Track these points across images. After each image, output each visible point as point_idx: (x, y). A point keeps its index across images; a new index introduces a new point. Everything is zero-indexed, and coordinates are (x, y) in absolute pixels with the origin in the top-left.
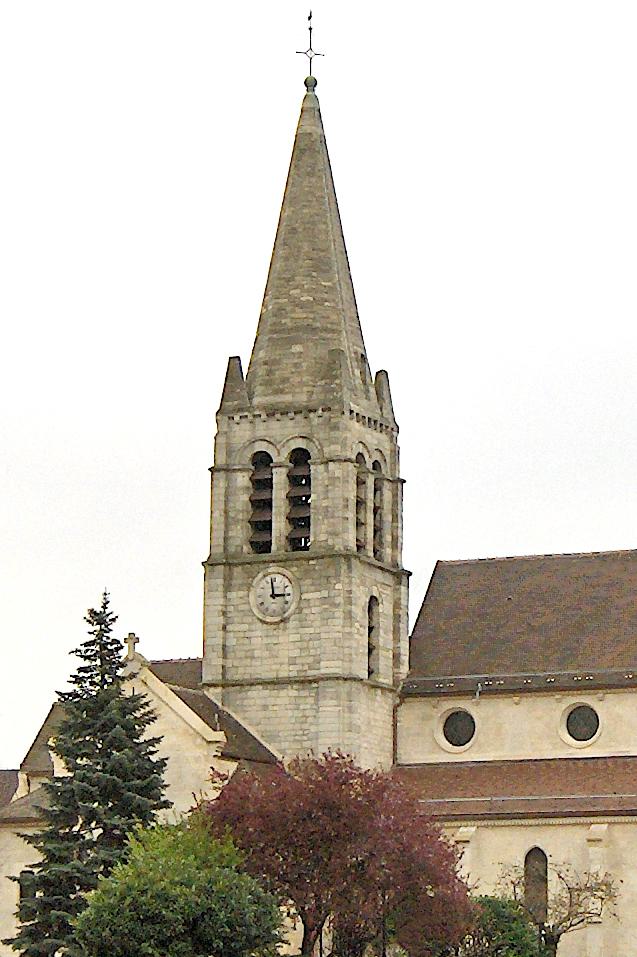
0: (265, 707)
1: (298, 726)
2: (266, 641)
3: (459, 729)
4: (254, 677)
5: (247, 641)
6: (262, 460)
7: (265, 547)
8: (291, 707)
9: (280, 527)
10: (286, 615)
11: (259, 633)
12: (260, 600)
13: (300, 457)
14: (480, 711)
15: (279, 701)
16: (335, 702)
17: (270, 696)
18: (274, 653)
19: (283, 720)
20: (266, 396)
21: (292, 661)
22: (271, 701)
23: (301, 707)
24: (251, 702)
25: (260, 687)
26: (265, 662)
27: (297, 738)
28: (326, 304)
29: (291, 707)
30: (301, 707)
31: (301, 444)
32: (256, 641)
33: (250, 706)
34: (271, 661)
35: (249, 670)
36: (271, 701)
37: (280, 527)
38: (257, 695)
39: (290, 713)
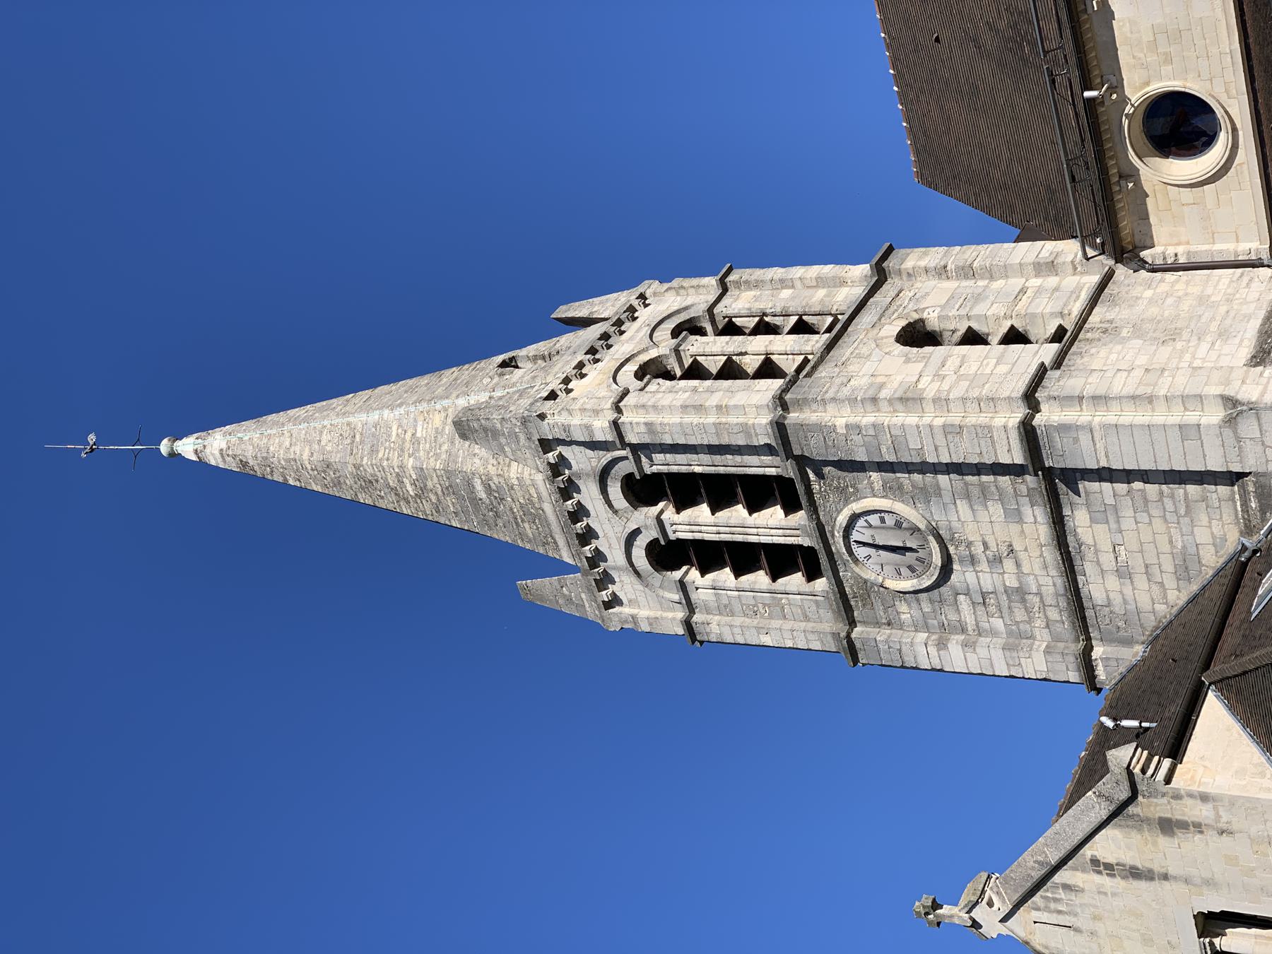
0: (1124, 573)
1: (1155, 512)
2: (984, 566)
3: (1180, 124)
4: (1062, 591)
5: (991, 600)
6: (668, 554)
7: (809, 552)
8: (1111, 519)
9: (772, 525)
10: (922, 526)
11: (970, 577)
12: (905, 571)
13: (643, 490)
14: (1142, 78)
15: (1105, 546)
16: (1084, 439)
17: (1098, 563)
18: (1004, 550)
19: (1146, 536)
20: (555, 542)
21: (1015, 516)
22: (1107, 560)
23: (1110, 500)
24: (1117, 599)
25: (1080, 579)
26: (1026, 569)
27: (1182, 512)
28: (419, 435)
29: (1111, 519)
30: (1110, 500)
31: (615, 490)
32: (988, 581)
33: (1125, 602)
34: (1022, 556)
35: (1049, 600)
36: (1107, 560)
37: (772, 525)
38: (1097, 588)
39: (1128, 523)
